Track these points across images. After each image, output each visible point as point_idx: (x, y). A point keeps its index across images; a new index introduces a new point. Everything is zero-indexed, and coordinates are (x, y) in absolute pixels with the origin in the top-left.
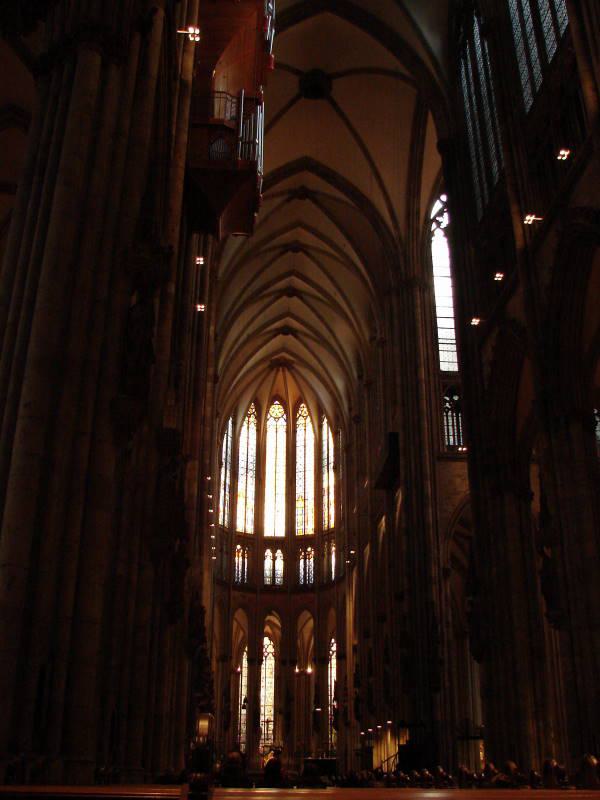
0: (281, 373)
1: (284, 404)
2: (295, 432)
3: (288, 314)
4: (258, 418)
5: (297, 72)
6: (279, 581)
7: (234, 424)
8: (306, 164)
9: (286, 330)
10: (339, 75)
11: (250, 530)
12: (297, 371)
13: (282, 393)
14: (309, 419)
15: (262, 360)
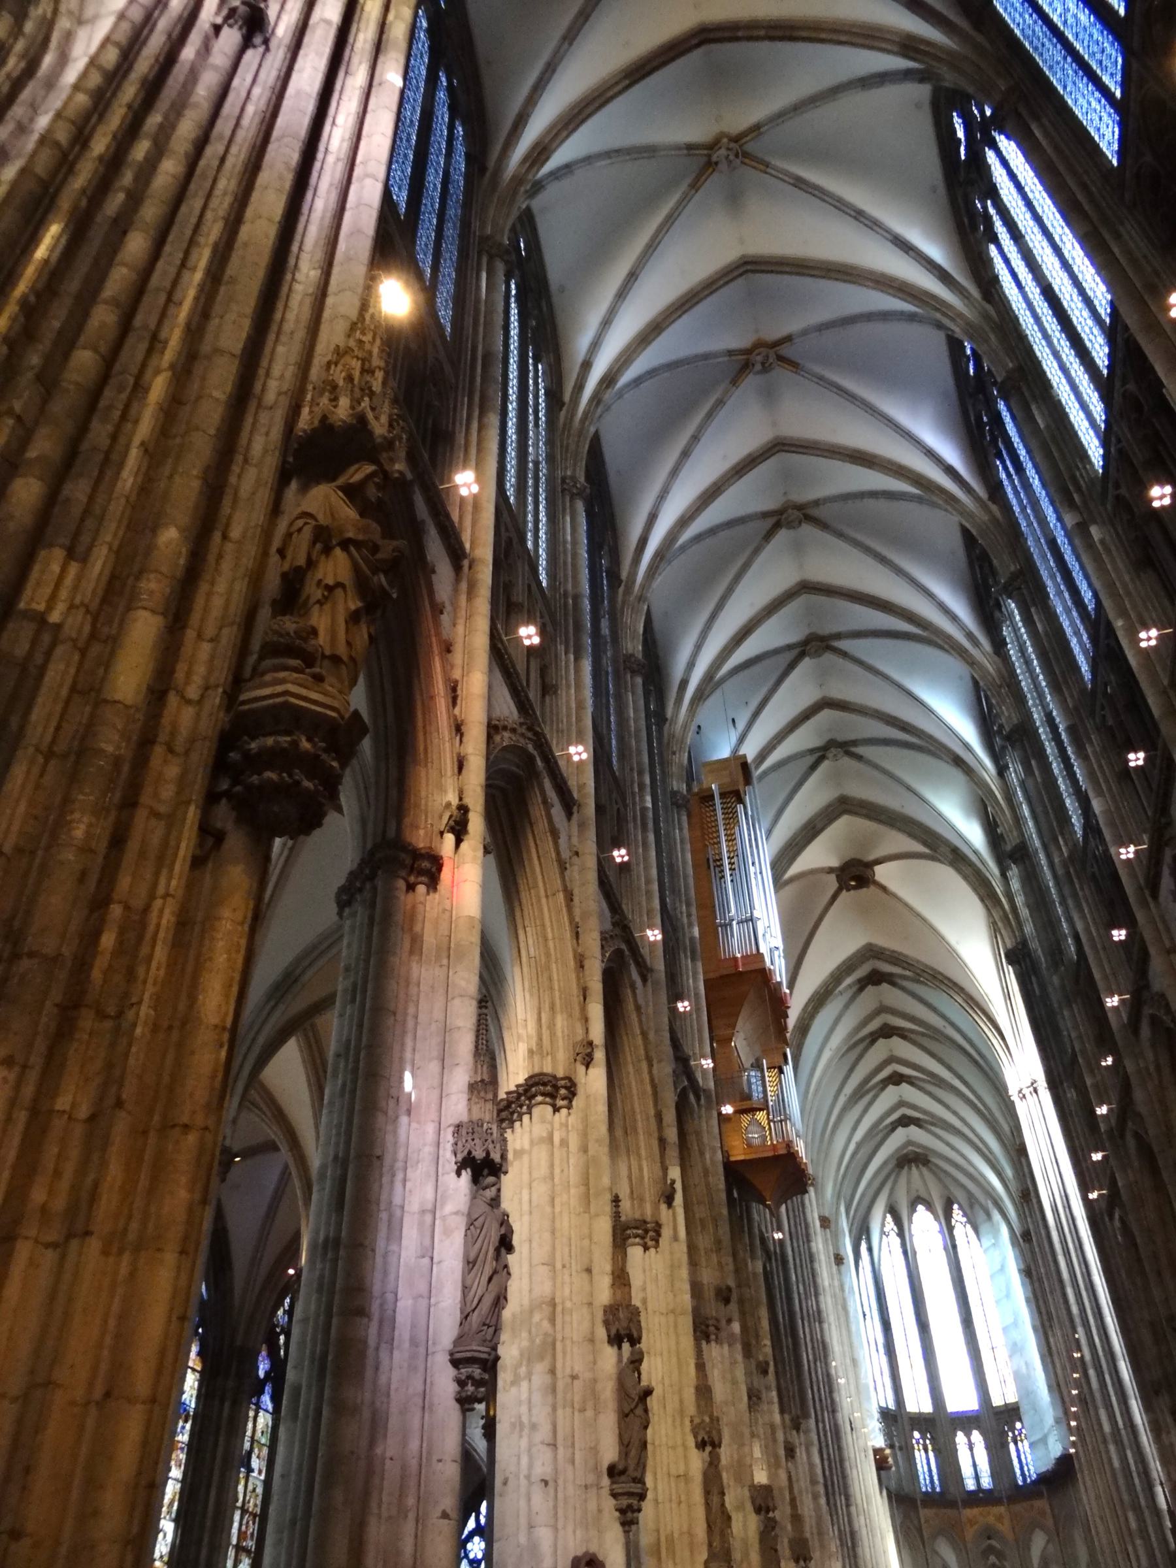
0: (914, 1168)
1: (930, 1207)
2: (954, 1247)
3: (902, 1104)
4: (901, 1234)
5: (831, 870)
6: (986, 1482)
7: (870, 1249)
8: (870, 952)
9: (905, 1121)
10: (879, 862)
11: (927, 1407)
12: (937, 1166)
13: (924, 1194)
14: (968, 1226)
15: (885, 1163)
